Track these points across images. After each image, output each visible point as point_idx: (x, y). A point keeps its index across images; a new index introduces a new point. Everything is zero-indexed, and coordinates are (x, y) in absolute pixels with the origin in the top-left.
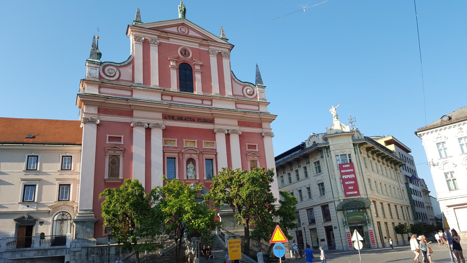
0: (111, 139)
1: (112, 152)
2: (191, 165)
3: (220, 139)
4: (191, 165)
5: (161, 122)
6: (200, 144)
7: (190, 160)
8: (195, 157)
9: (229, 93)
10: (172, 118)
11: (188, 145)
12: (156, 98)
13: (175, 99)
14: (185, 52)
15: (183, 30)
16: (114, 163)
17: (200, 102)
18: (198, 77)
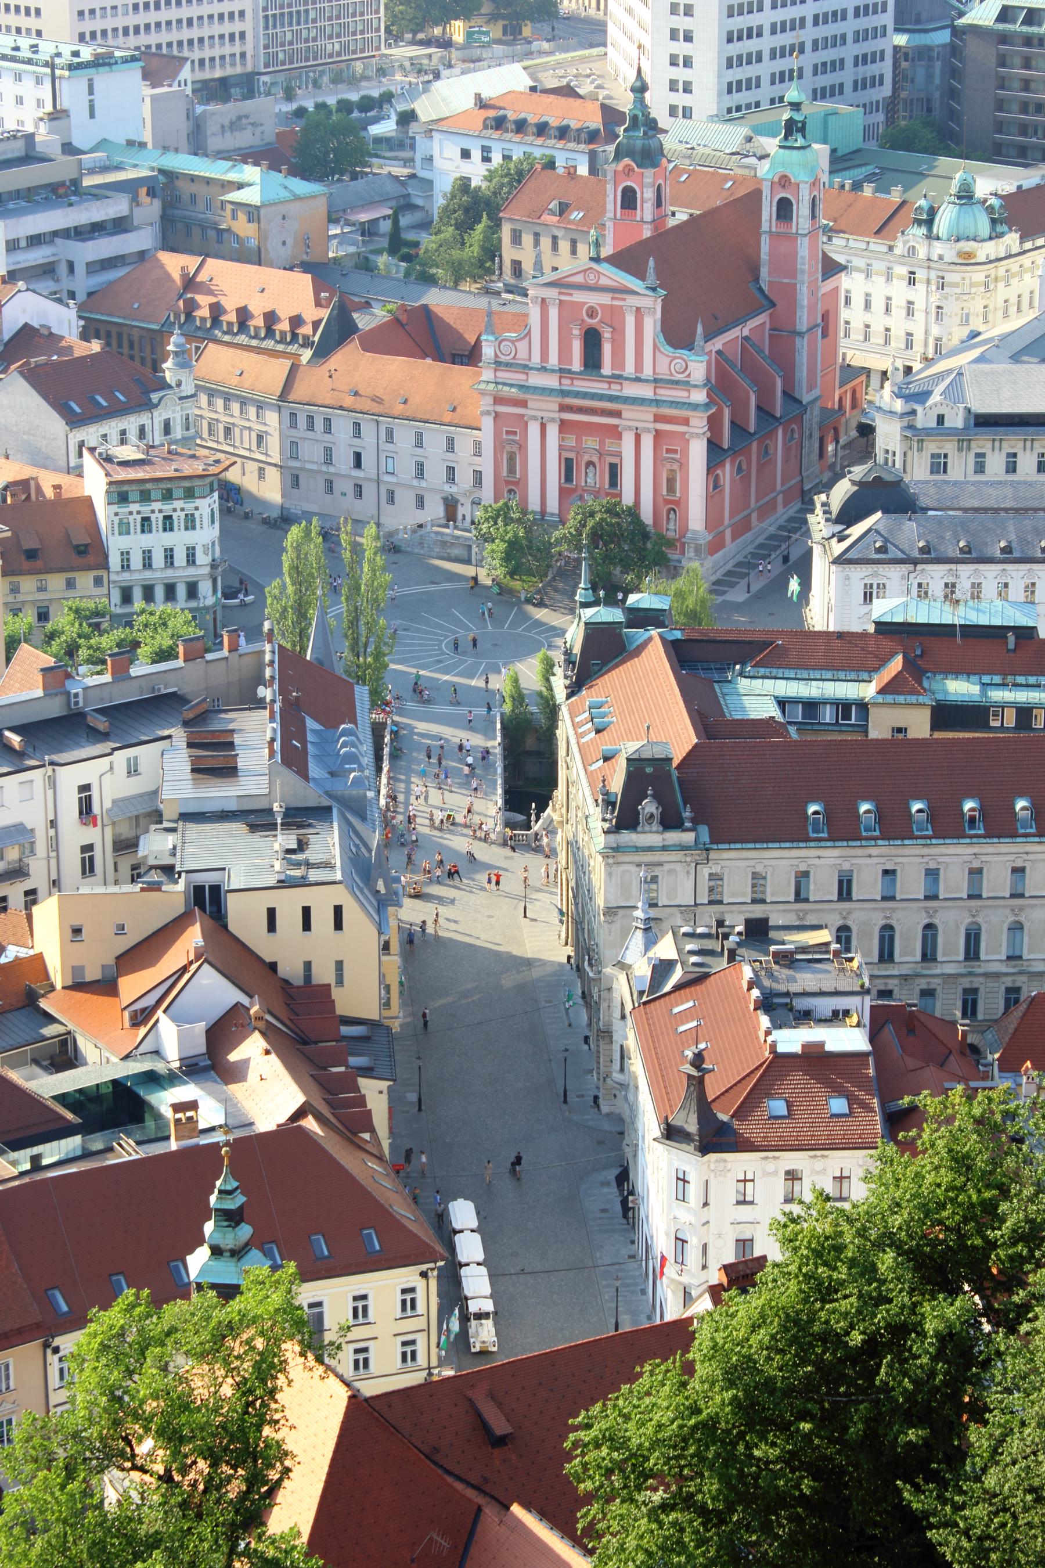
0: (507, 432)
1: (508, 448)
2: (591, 468)
3: (628, 439)
4: (591, 468)
5: (556, 415)
6: (602, 443)
7: (590, 463)
8: (595, 459)
9: (648, 372)
10: (570, 409)
11: (591, 443)
12: (551, 382)
13: (576, 382)
14: (592, 313)
15: (592, 276)
16: (512, 459)
17: (606, 386)
18: (607, 349)
